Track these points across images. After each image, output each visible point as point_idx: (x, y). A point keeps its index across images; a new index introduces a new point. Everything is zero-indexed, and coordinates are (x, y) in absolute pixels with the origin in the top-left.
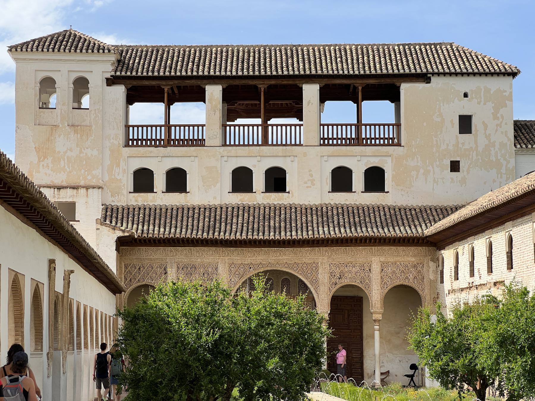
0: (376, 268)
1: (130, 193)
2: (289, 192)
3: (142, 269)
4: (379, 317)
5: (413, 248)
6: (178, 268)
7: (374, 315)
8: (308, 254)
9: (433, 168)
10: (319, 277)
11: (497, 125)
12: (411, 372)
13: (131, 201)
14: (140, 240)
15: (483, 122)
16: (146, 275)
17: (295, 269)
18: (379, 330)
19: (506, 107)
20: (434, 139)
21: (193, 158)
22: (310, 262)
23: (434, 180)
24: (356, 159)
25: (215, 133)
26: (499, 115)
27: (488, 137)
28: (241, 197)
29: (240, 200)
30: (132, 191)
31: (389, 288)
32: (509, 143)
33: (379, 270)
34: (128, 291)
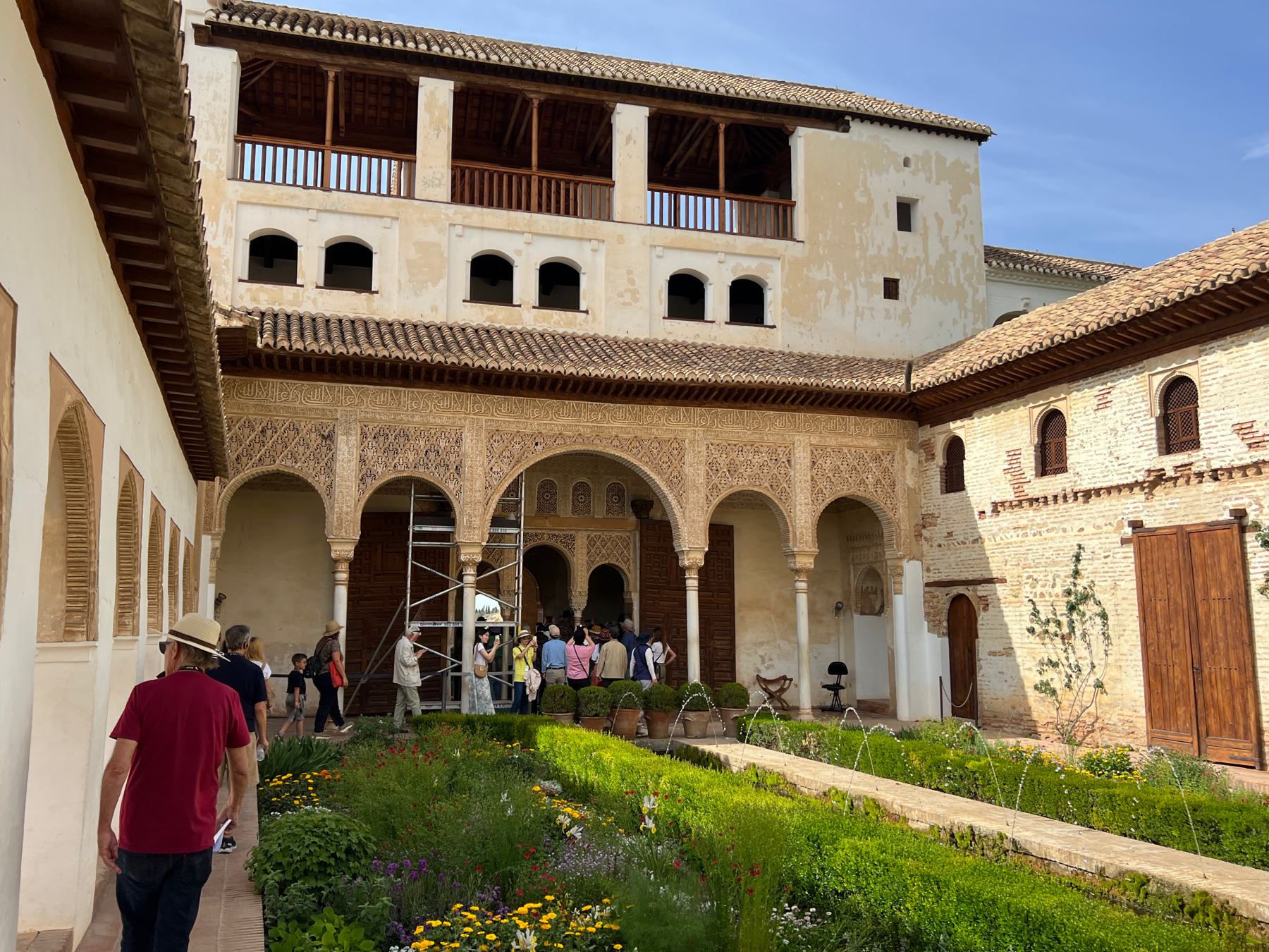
0: (802, 457)
1: (240, 280)
2: (587, 312)
3: (269, 433)
4: (807, 562)
5: (874, 420)
6: (364, 435)
7: (798, 559)
8: (663, 421)
9: (855, 287)
10: (686, 471)
11: (958, 223)
12: (832, 679)
13: (241, 297)
14: (269, 357)
15: (936, 214)
16: (279, 447)
17: (635, 451)
18: (809, 591)
19: (970, 193)
20: (857, 234)
21: (388, 220)
22: (666, 437)
23: (857, 310)
24: (716, 258)
25: (439, 176)
26: (960, 206)
27: (944, 241)
28: (491, 313)
29: (488, 319)
30: (246, 277)
31: (828, 501)
32: (976, 257)
33: (808, 462)
34: (235, 481)
